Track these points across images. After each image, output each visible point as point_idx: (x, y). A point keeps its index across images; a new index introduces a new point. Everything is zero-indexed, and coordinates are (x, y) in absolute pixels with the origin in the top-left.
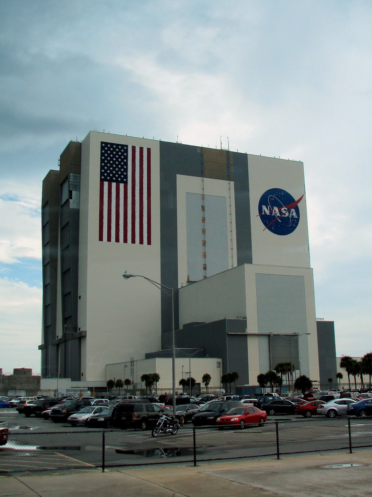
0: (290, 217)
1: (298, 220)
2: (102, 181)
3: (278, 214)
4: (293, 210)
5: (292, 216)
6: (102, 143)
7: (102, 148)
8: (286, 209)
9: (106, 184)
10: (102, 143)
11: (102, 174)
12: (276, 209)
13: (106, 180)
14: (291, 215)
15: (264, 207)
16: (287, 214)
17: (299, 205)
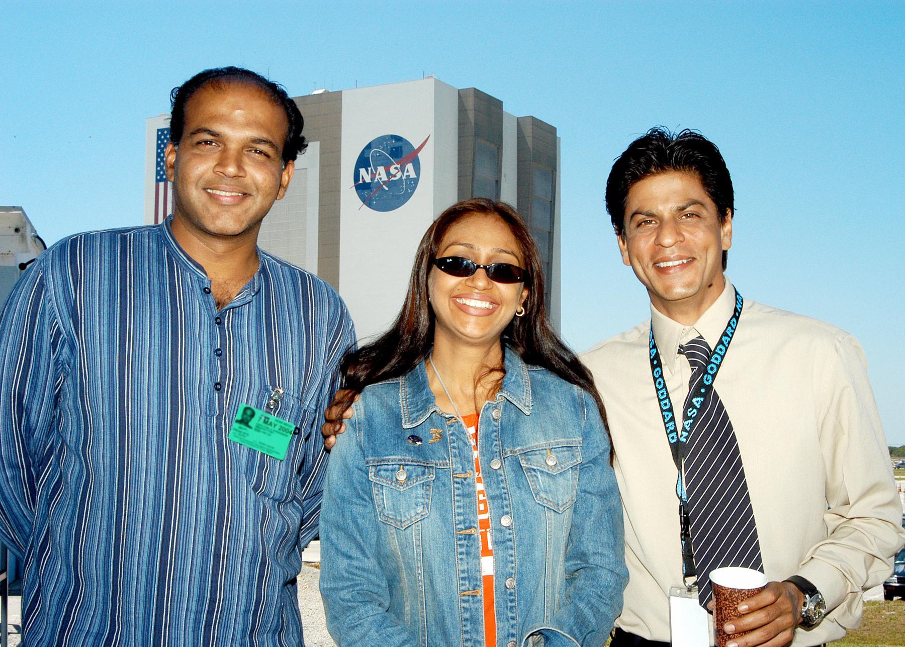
0: (404, 177)
1: (416, 181)
2: (158, 181)
3: (385, 178)
4: (410, 166)
5: (408, 176)
6: (158, 130)
7: (159, 138)
8: (399, 166)
9: (162, 184)
10: (158, 130)
11: (158, 173)
12: (381, 169)
13: (161, 180)
14: (406, 174)
15: (363, 171)
16: (399, 175)
17: (420, 155)
